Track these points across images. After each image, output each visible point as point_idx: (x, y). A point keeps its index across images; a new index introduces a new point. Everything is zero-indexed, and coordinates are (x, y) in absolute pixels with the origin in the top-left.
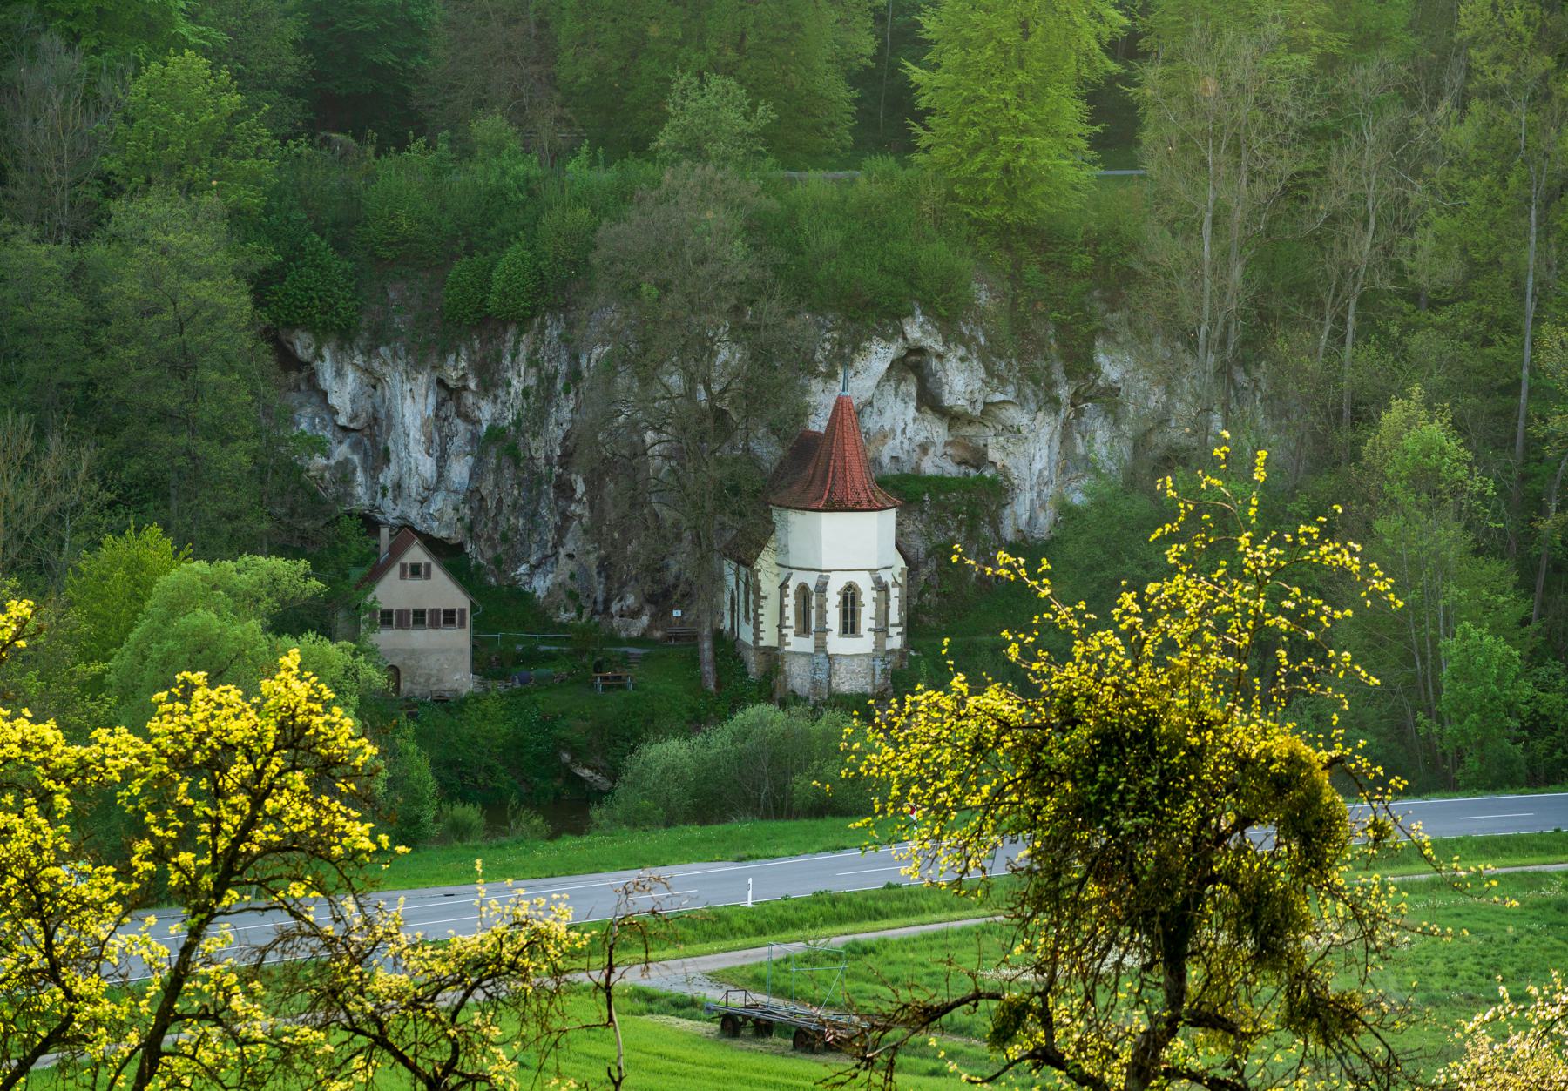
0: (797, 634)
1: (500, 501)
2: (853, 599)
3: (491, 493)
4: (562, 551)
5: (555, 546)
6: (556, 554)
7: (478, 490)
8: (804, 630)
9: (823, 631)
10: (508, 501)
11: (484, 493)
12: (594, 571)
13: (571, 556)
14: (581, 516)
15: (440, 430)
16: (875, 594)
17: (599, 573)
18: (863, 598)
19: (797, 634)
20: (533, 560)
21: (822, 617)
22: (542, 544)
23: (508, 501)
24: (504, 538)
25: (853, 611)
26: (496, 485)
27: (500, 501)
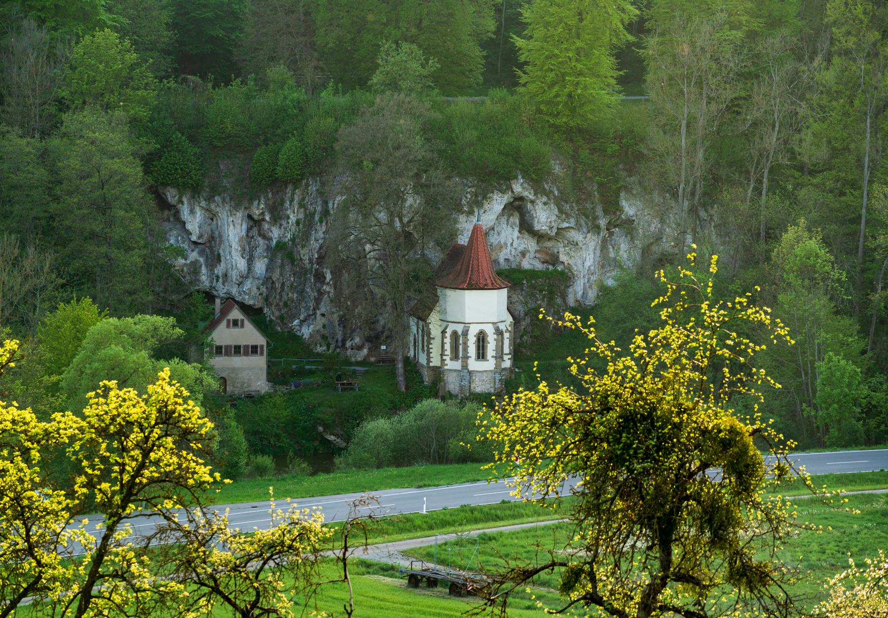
0: (451, 359)
1: (283, 284)
2: (483, 339)
3: (278, 279)
4: (318, 312)
5: (314, 309)
6: (315, 314)
7: (271, 278)
8: (455, 357)
9: (466, 357)
10: (288, 284)
11: (274, 279)
12: (337, 323)
13: (323, 315)
14: (329, 292)
15: (249, 244)
16: (495, 336)
17: (339, 325)
18: (489, 339)
19: (451, 359)
20: (302, 317)
21: (465, 349)
22: (307, 308)
23: (288, 284)
24: (286, 305)
25: (483, 346)
26: (281, 275)
27: (283, 284)
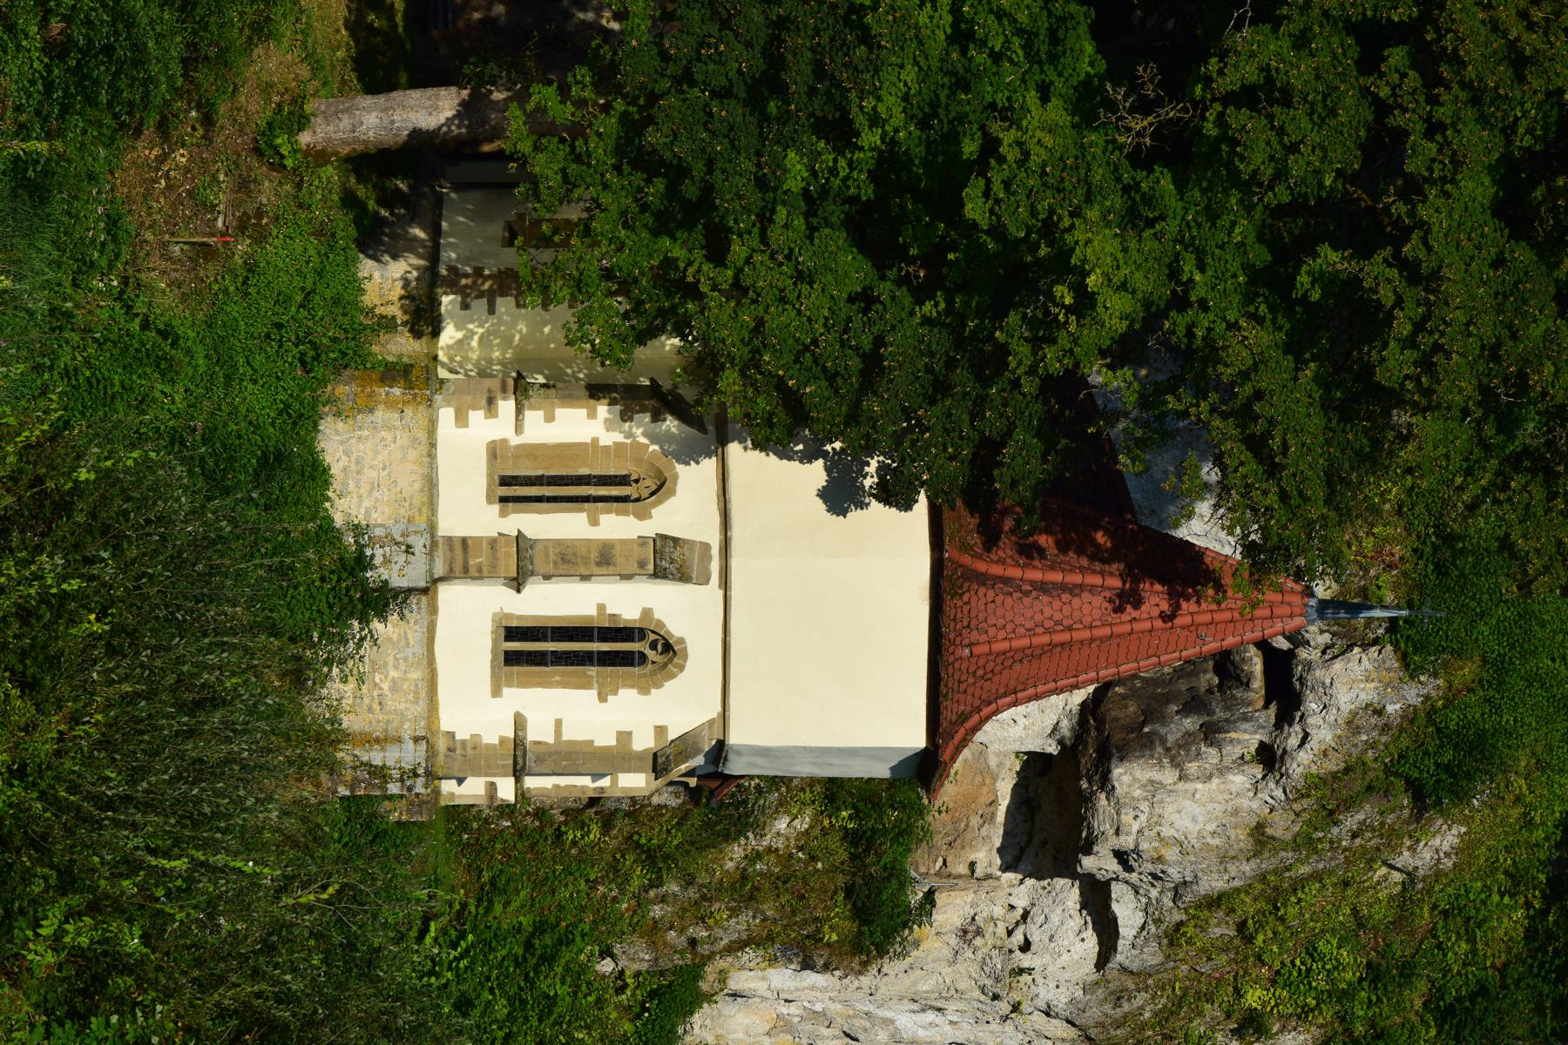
0: (495, 451)
2: (625, 659)
18: (627, 695)
19: (495, 451)
